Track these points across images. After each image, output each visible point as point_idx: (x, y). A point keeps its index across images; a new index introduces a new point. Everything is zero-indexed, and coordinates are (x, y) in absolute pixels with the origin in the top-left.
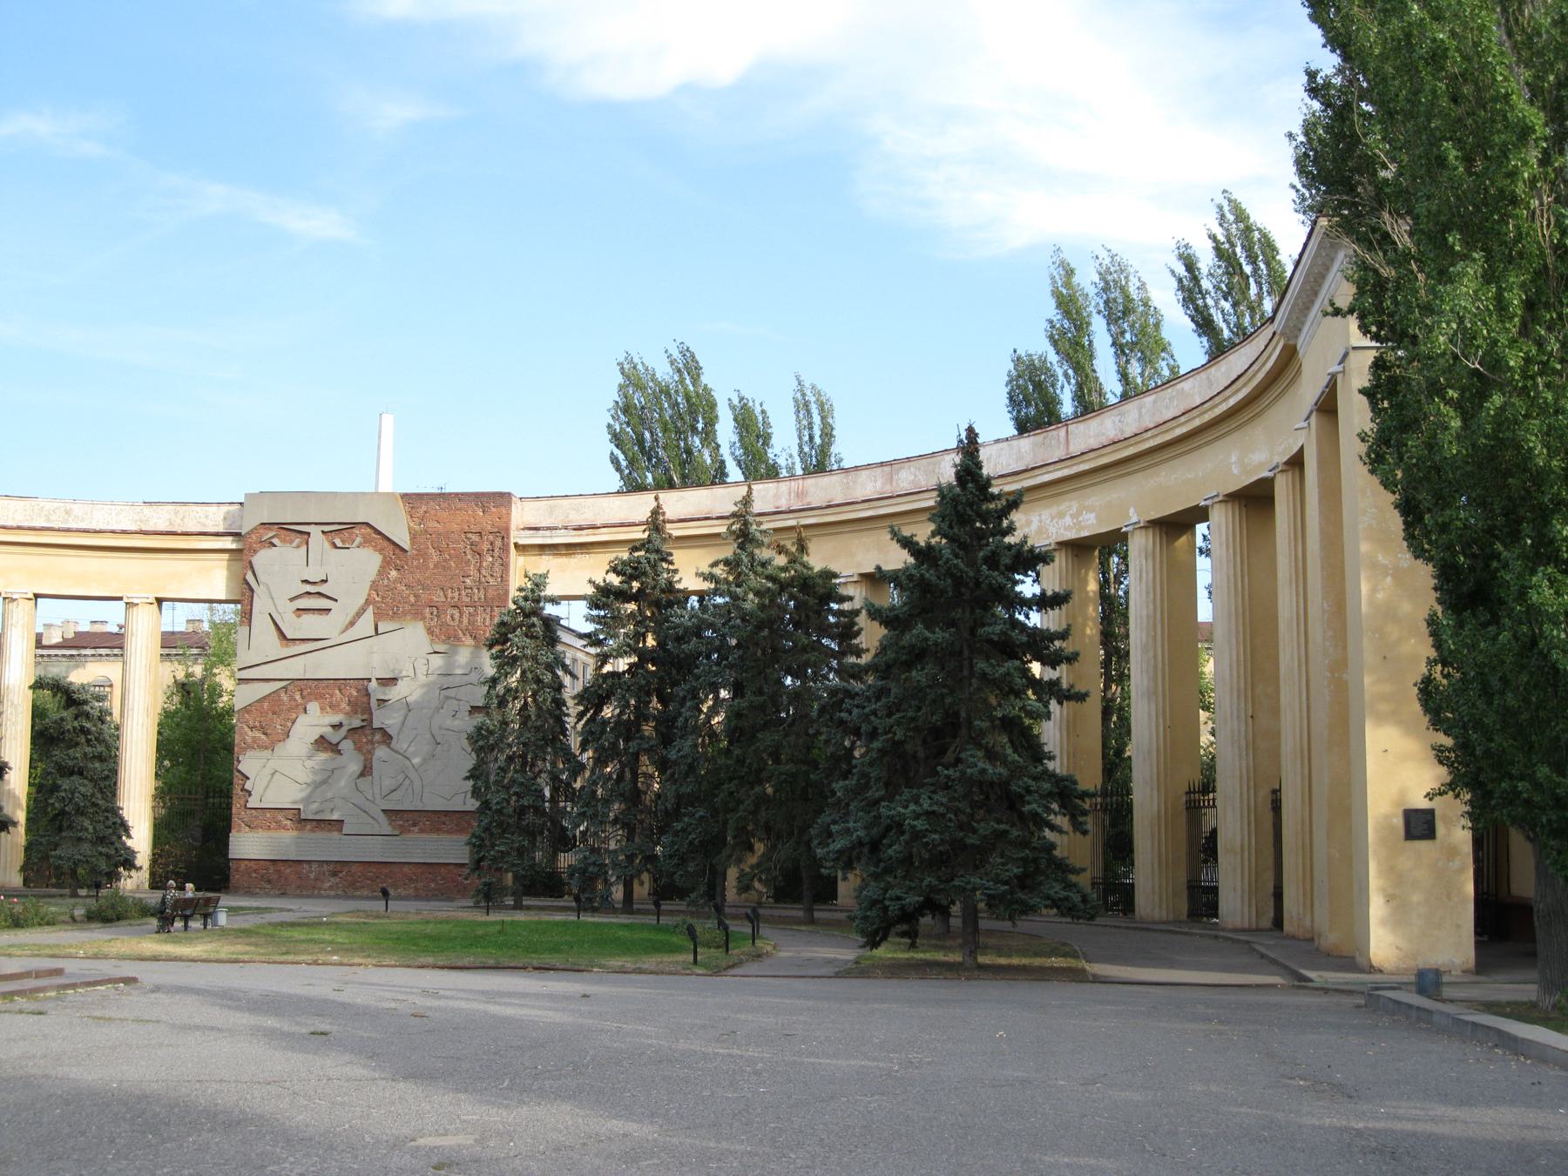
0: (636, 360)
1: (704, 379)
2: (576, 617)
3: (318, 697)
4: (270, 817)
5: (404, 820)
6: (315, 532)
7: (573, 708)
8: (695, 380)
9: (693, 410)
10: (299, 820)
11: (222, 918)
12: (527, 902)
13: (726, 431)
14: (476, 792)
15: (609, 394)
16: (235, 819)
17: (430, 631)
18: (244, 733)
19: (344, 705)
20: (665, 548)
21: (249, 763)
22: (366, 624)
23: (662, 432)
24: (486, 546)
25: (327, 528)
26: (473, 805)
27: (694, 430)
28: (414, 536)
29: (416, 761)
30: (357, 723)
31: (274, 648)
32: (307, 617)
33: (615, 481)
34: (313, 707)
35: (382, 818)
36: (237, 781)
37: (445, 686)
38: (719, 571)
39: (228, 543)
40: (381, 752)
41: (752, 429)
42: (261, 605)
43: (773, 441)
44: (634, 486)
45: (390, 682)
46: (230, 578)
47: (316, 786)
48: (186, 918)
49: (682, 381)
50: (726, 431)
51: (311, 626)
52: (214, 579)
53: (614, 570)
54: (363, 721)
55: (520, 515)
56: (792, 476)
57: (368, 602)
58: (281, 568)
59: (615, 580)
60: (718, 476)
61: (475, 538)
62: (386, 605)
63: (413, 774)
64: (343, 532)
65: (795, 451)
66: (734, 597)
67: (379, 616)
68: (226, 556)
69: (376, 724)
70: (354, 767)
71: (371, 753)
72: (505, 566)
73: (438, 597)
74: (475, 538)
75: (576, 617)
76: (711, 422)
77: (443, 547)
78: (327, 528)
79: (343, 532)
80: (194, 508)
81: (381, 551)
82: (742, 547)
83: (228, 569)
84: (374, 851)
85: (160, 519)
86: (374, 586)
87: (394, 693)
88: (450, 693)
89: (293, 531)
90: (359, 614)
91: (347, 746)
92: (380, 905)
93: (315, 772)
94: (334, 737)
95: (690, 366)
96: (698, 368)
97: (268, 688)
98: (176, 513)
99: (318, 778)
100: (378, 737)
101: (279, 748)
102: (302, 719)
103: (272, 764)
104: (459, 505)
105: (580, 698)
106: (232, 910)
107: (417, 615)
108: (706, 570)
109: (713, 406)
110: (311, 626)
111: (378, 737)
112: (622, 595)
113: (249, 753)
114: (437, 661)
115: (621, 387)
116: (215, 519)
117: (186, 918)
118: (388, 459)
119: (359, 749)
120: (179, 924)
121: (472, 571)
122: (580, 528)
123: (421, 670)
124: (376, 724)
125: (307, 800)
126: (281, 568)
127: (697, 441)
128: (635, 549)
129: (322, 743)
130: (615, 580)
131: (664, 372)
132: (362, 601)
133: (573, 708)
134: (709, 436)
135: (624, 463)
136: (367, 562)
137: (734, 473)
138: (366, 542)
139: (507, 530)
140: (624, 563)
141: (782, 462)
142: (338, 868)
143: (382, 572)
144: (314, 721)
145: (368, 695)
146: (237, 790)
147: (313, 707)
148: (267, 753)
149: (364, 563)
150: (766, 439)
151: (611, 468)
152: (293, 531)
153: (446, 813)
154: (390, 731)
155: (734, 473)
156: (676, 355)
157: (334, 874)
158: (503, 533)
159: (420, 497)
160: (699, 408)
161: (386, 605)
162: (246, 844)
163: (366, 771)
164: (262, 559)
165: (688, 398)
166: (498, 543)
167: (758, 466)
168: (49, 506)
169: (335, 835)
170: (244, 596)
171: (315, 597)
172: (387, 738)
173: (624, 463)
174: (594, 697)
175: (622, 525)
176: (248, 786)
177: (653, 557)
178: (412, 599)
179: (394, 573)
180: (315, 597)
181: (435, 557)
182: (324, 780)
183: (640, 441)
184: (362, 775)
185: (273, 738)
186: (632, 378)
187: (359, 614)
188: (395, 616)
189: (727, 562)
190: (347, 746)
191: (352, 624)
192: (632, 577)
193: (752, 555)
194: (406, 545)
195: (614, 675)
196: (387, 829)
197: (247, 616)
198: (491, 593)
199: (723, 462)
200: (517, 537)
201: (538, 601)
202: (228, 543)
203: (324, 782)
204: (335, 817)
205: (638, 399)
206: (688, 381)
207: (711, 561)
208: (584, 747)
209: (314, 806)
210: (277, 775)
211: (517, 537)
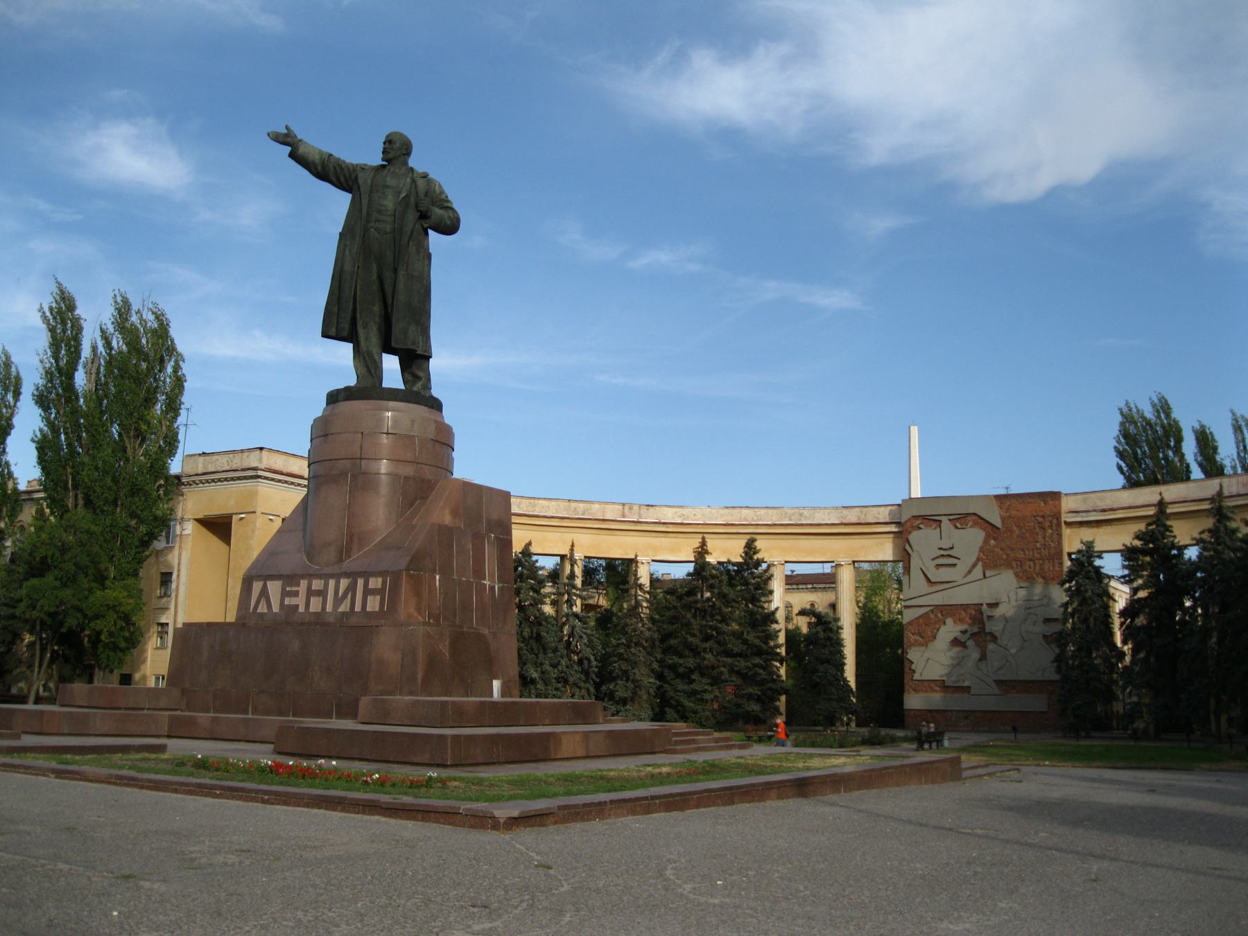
0: (1132, 406)
1: (1173, 415)
2: (1112, 565)
3: (953, 615)
4: (927, 685)
5: (1006, 686)
6: (945, 520)
7: (1117, 621)
8: (1168, 416)
9: (1167, 434)
10: (943, 686)
11: (946, 743)
12: (1093, 734)
13: (1190, 448)
14: (1059, 670)
15: (1115, 430)
16: (906, 687)
17: (1016, 575)
18: (909, 637)
19: (967, 620)
20: (1169, 523)
21: (914, 655)
22: (978, 571)
23: (1149, 448)
24: (1047, 524)
26: (1057, 677)
27: (1169, 447)
28: (1003, 519)
29: (1013, 651)
30: (976, 630)
32: (943, 569)
33: (1120, 481)
35: (993, 685)
36: (906, 664)
37: (1028, 607)
38: (1206, 536)
39: (893, 528)
40: (991, 646)
41: (1205, 442)
42: (915, 563)
43: (1220, 450)
44: (1132, 484)
45: (994, 605)
46: (894, 549)
47: (954, 666)
48: (930, 743)
49: (1159, 417)
50: (1190, 448)
51: (945, 574)
52: (884, 550)
53: (1137, 537)
54: (979, 627)
55: (1067, 504)
56: (1235, 474)
57: (978, 559)
58: (925, 542)
59: (1138, 543)
60: (1185, 476)
61: (1040, 519)
62: (989, 561)
65: (1235, 457)
66: (1216, 551)
67: (985, 567)
69: (988, 630)
70: (976, 655)
71: (986, 647)
72: (1060, 535)
73: (1020, 555)
74: (1040, 519)
75: (1112, 565)
76: (1179, 440)
77: (1021, 527)
81: (984, 529)
82: (1219, 521)
83: (894, 543)
84: (990, 704)
85: (852, 517)
86: (981, 550)
87: (998, 612)
88: (1032, 611)
89: (931, 520)
90: (974, 566)
91: (970, 643)
92: (1012, 736)
93: (952, 658)
94: (963, 638)
95: (1163, 407)
96: (1169, 408)
97: (922, 611)
99: (955, 662)
100: (988, 638)
101: (931, 646)
102: (943, 629)
103: (927, 655)
105: (1123, 613)
106: (950, 739)
107: (1008, 564)
108: (1197, 536)
109: (1179, 430)
110: (945, 574)
112: (1144, 552)
113: (913, 649)
114: (1022, 593)
115: (1122, 424)
116: (883, 515)
117: (930, 743)
118: (983, 476)
119: (977, 644)
120: (926, 746)
121: (1040, 539)
122: (1104, 511)
123: (1013, 597)
124: (988, 630)
125: (949, 675)
126: (925, 542)
127: (1171, 453)
128: (1149, 524)
129: (956, 642)
130: (1138, 543)
131: (1149, 414)
132: (974, 559)
133: (1117, 621)
134: (1178, 449)
135: (1125, 469)
137: (1196, 473)
138: (975, 524)
139: (1060, 513)
140: (1144, 533)
141: (1227, 462)
142: (968, 714)
143: (986, 541)
144: (950, 630)
145: (981, 613)
146: (907, 670)
147: (949, 621)
149: (975, 536)
150: (1215, 449)
151: (1118, 473)
152: (931, 520)
153: (1033, 682)
154: (997, 634)
155: (1196, 473)
156: (1156, 401)
157: (966, 718)
158: (1057, 515)
160: (1173, 432)
161: (989, 561)
162: (913, 701)
163: (983, 657)
164: (914, 537)
165: (1163, 426)
166: (1055, 521)
167: (1212, 468)
168: (790, 512)
169: (966, 695)
170: (904, 557)
171: (947, 557)
172: (994, 638)
173: (1125, 469)
174: (1130, 612)
175: (1130, 508)
176: (913, 667)
177: (1162, 529)
179: (992, 542)
181: (1017, 531)
182: (958, 663)
183: (1135, 454)
184: (980, 660)
185: (927, 639)
186: (1128, 418)
187: (974, 566)
188: (995, 567)
189: (1210, 531)
191: (969, 572)
192: (1149, 542)
193: (1226, 527)
194: (998, 523)
195: (1140, 599)
196: (997, 691)
197: (907, 570)
198: (1052, 551)
199: (1188, 466)
200: (1066, 517)
201: (1091, 556)
202: (893, 528)
203: (959, 664)
204: (966, 684)
205: (1132, 430)
206: (1163, 416)
207: (1200, 530)
208: (1124, 642)
209: (953, 678)
210: (931, 661)
211: (1066, 517)
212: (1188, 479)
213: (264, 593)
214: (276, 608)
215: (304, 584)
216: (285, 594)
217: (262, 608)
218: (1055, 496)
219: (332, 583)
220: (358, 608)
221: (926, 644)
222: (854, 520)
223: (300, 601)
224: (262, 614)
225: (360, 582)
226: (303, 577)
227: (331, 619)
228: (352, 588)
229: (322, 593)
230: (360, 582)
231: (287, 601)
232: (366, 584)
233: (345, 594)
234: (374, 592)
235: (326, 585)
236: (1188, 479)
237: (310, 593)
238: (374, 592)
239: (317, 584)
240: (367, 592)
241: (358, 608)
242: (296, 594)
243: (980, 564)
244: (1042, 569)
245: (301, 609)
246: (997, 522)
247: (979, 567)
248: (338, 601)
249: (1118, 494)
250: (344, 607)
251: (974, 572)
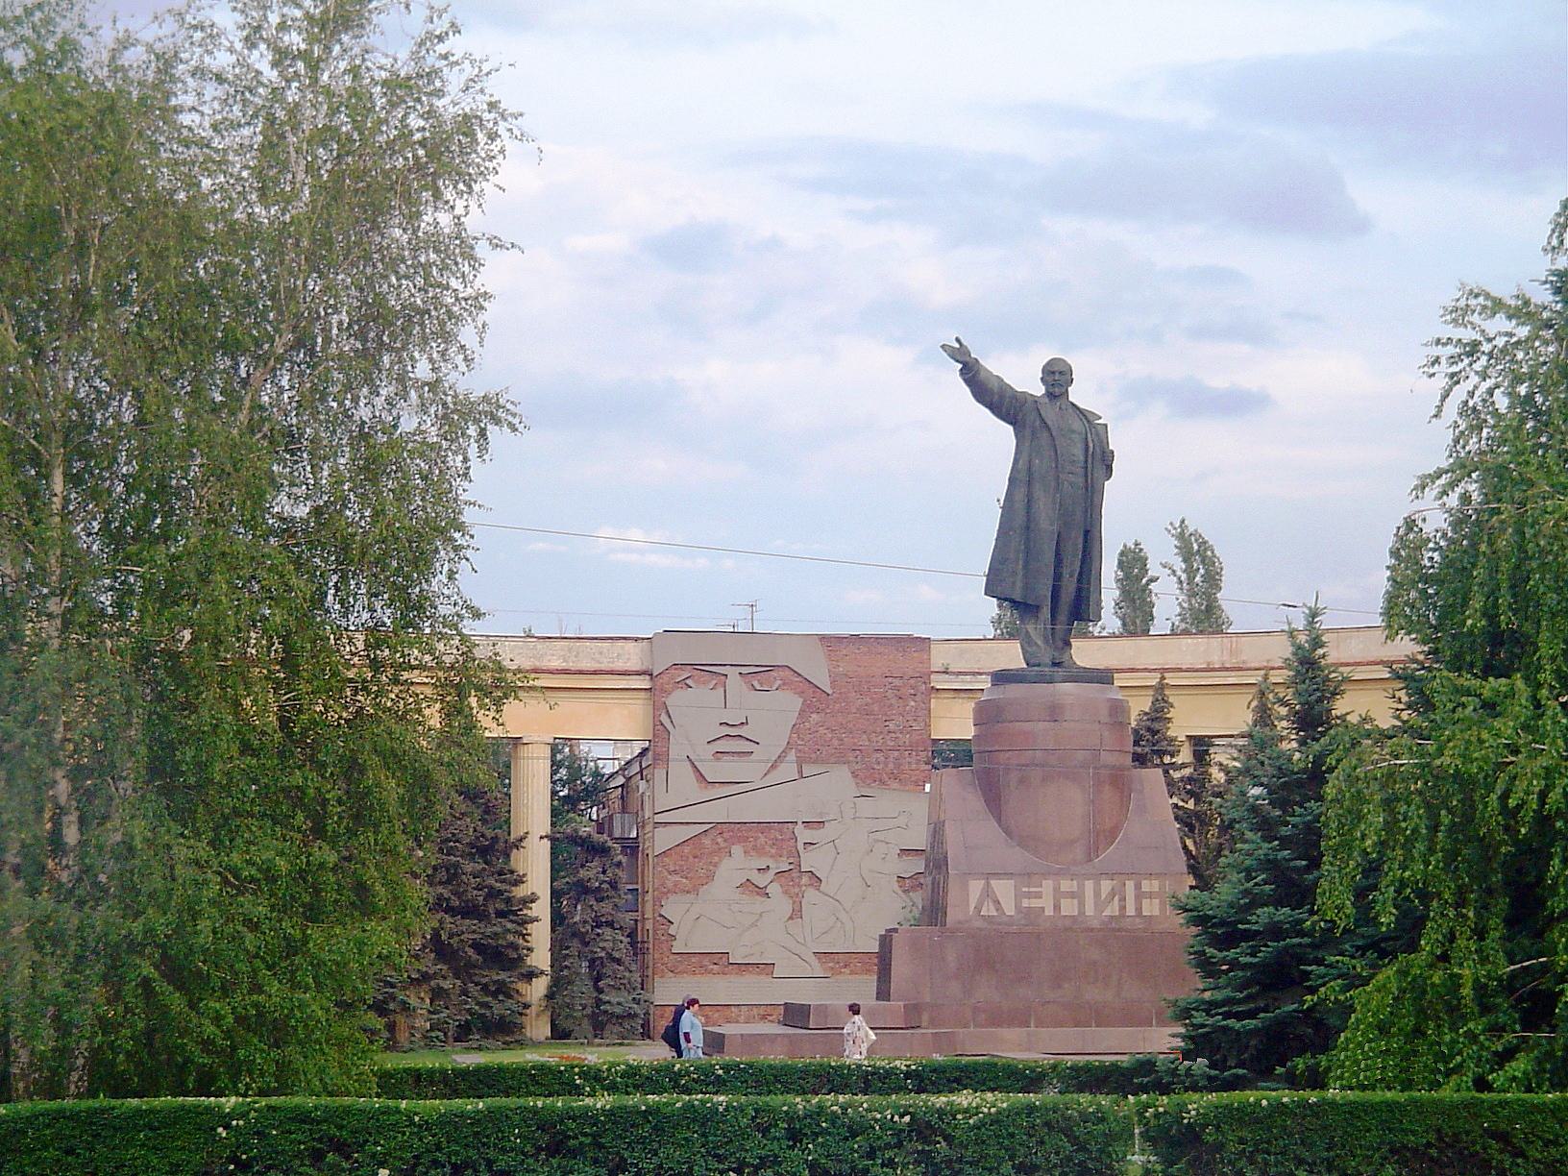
22: (788, 769)
25: (745, 670)
31: (693, 791)
34: (737, 850)
35: (813, 959)
39: (644, 683)
40: (811, 894)
42: (677, 749)
51: (728, 770)
55: (938, 658)
58: (696, 713)
61: (897, 682)
62: (809, 750)
63: (843, 916)
64: (760, 675)
68: (643, 694)
78: (745, 670)
79: (760, 675)
80: (588, 643)
89: (706, 672)
91: (774, 889)
94: (761, 880)
98: (570, 650)
100: (805, 880)
104: (881, 649)
107: (841, 759)
110: (728, 770)
111: (805, 880)
113: (672, 898)
136: (791, 703)
138: (785, 684)
147: (737, 850)
148: (692, 896)
152: (706, 672)
158: (925, 676)
159: (840, 639)
161: (809, 750)
163: (797, 913)
164: (677, 700)
169: (765, 979)
171: (734, 737)
178: (836, 742)
180: (734, 737)
190: (774, 889)
212: (1146, 633)
213: (987, 893)
214: (1010, 909)
215: (1048, 885)
216: (1019, 896)
217: (989, 910)
218: (925, 642)
219: (1089, 885)
220: (1131, 911)
221: (694, 890)
222: (556, 663)
223: (1046, 904)
224: (989, 919)
225: (1130, 885)
226: (1045, 875)
227: (1096, 924)
228: (1118, 893)
229: (1078, 896)
230: (1130, 885)
231: (1025, 903)
232: (1138, 886)
233: (1112, 894)
234: (1151, 895)
235: (1081, 887)
236: (1146, 633)
237: (1058, 895)
238: (1151, 895)
239: (1066, 885)
240: (1139, 896)
241: (1131, 911)
242: (1038, 895)
243: (792, 756)
244: (898, 766)
245: (1049, 912)
246: (823, 681)
247: (792, 756)
248: (1099, 905)
249: (989, 644)
250: (1112, 910)
251: (782, 766)
